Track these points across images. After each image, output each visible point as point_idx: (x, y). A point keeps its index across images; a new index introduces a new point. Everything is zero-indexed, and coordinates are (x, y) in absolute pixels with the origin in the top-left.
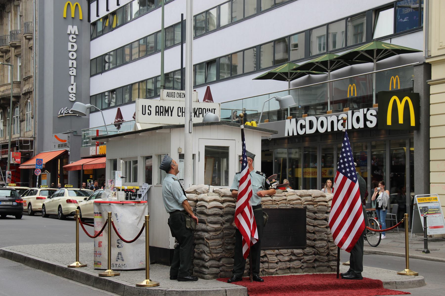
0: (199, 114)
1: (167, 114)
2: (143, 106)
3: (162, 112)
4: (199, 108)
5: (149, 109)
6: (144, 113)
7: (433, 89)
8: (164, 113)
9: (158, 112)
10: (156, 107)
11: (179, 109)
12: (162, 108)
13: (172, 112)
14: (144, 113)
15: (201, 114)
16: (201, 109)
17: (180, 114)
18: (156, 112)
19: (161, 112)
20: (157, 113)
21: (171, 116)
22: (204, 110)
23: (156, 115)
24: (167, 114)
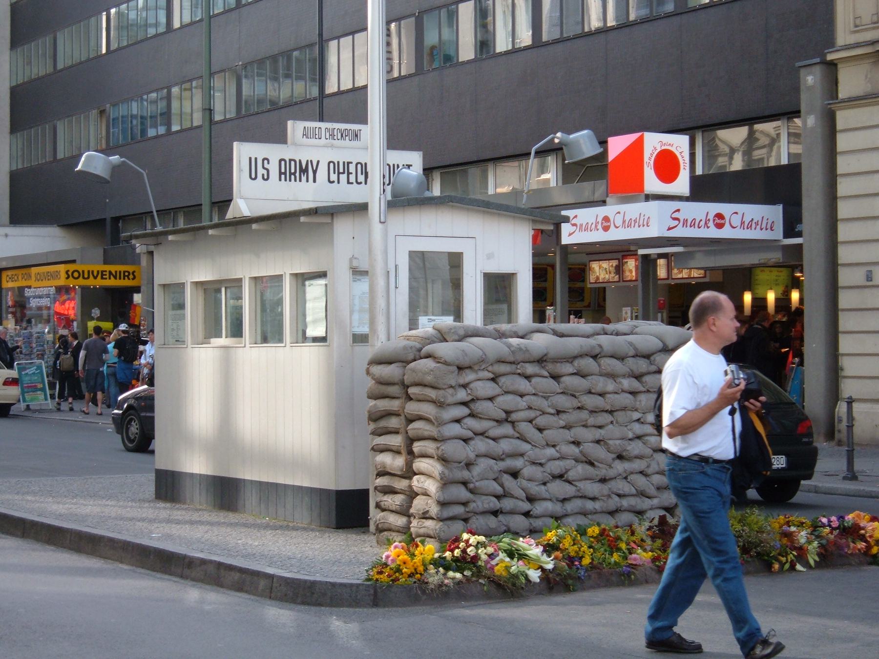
1: (304, 178)
2: (250, 159)
3: (294, 174)
5: (264, 168)
6: (253, 176)
7: (843, 118)
8: (298, 174)
9: (285, 173)
10: (280, 161)
11: (332, 165)
12: (293, 163)
13: (315, 172)
14: (253, 176)
17: (334, 177)
18: (281, 173)
19: (291, 174)
20: (283, 176)
21: (315, 181)
23: (280, 180)
24: (304, 178)
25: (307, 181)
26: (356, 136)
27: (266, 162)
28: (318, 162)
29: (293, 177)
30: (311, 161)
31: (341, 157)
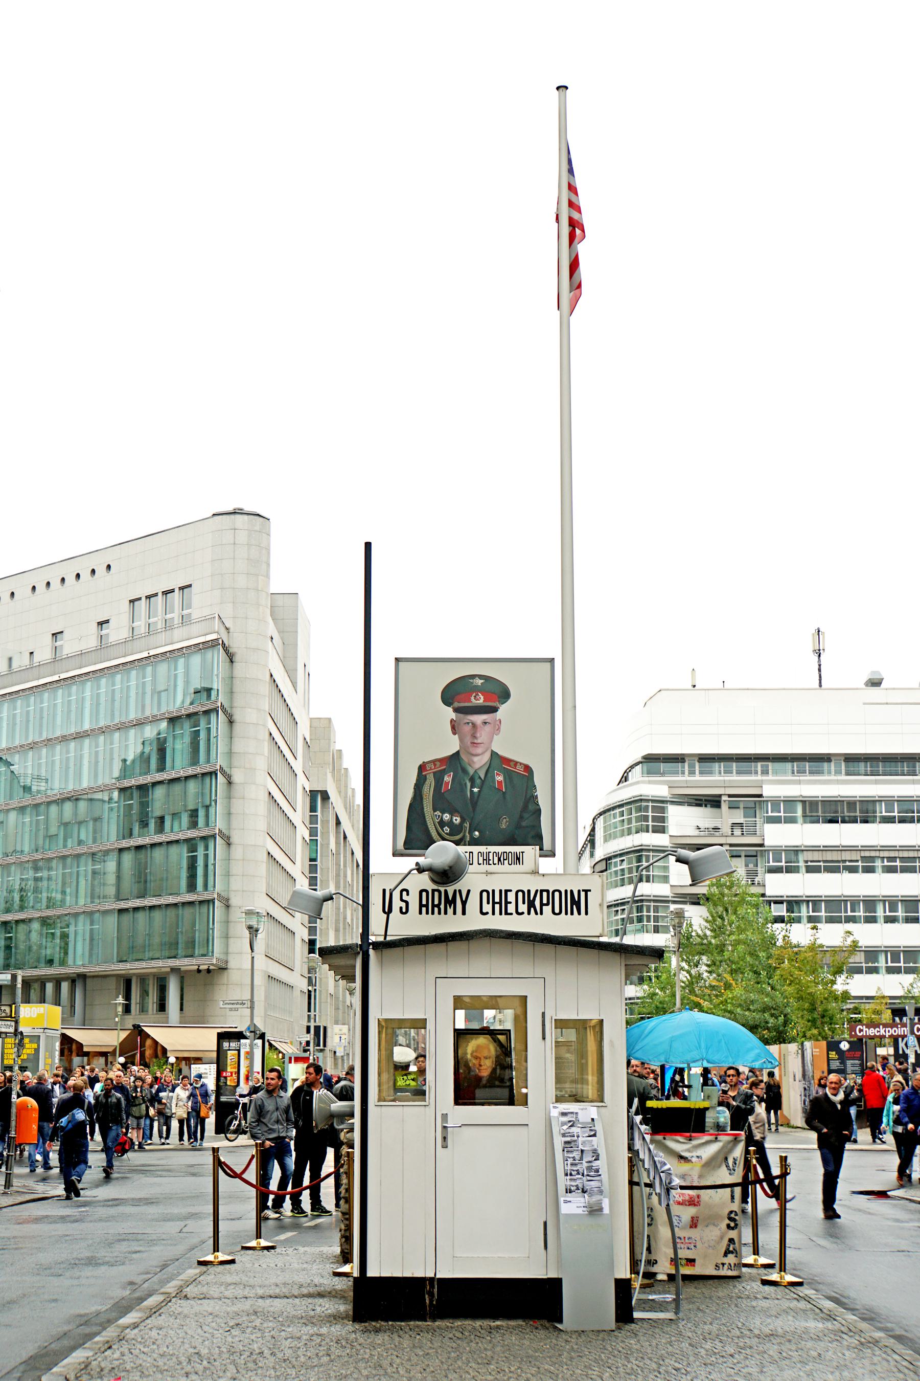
0: (542, 905)
1: (450, 911)
3: (438, 906)
4: (542, 891)
5: (402, 900)
8: (442, 907)
9: (427, 906)
10: (421, 892)
11: (485, 894)
13: (464, 903)
15: (548, 904)
16: (548, 891)
17: (487, 908)
18: (421, 906)
19: (433, 906)
20: (424, 909)
21: (464, 913)
22: (557, 894)
23: (420, 913)
24: (450, 911)
25: (455, 913)
26: (518, 859)
27: (404, 893)
28: (469, 891)
29: (436, 909)
30: (460, 891)
31: (496, 884)
